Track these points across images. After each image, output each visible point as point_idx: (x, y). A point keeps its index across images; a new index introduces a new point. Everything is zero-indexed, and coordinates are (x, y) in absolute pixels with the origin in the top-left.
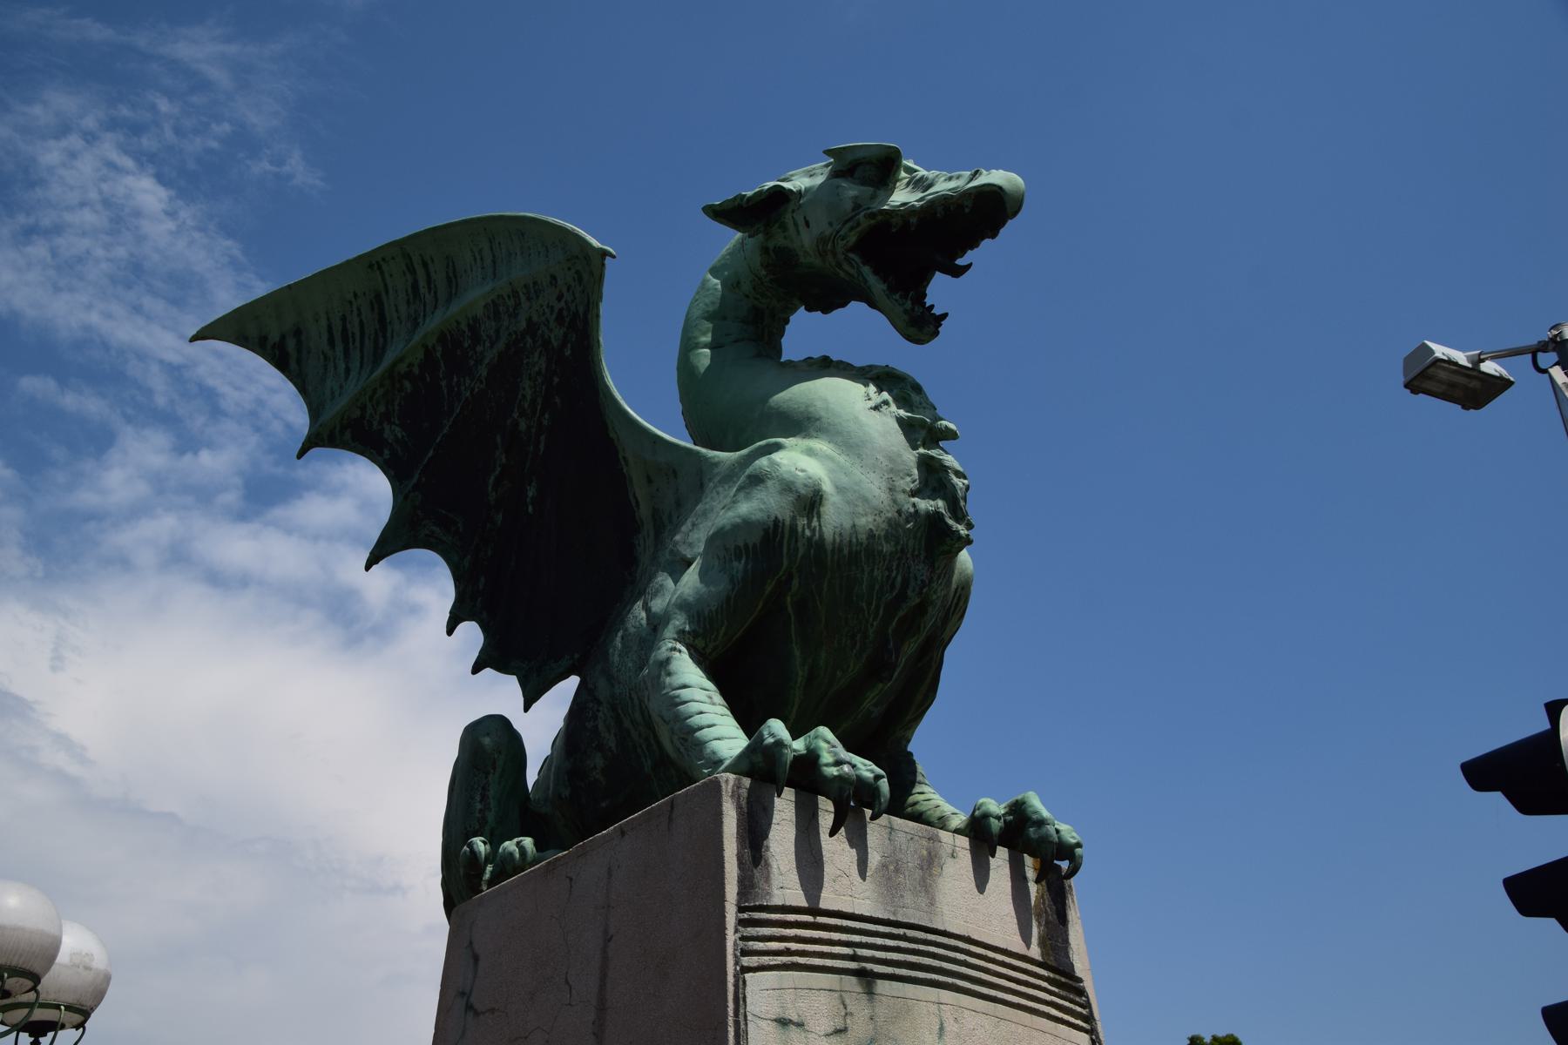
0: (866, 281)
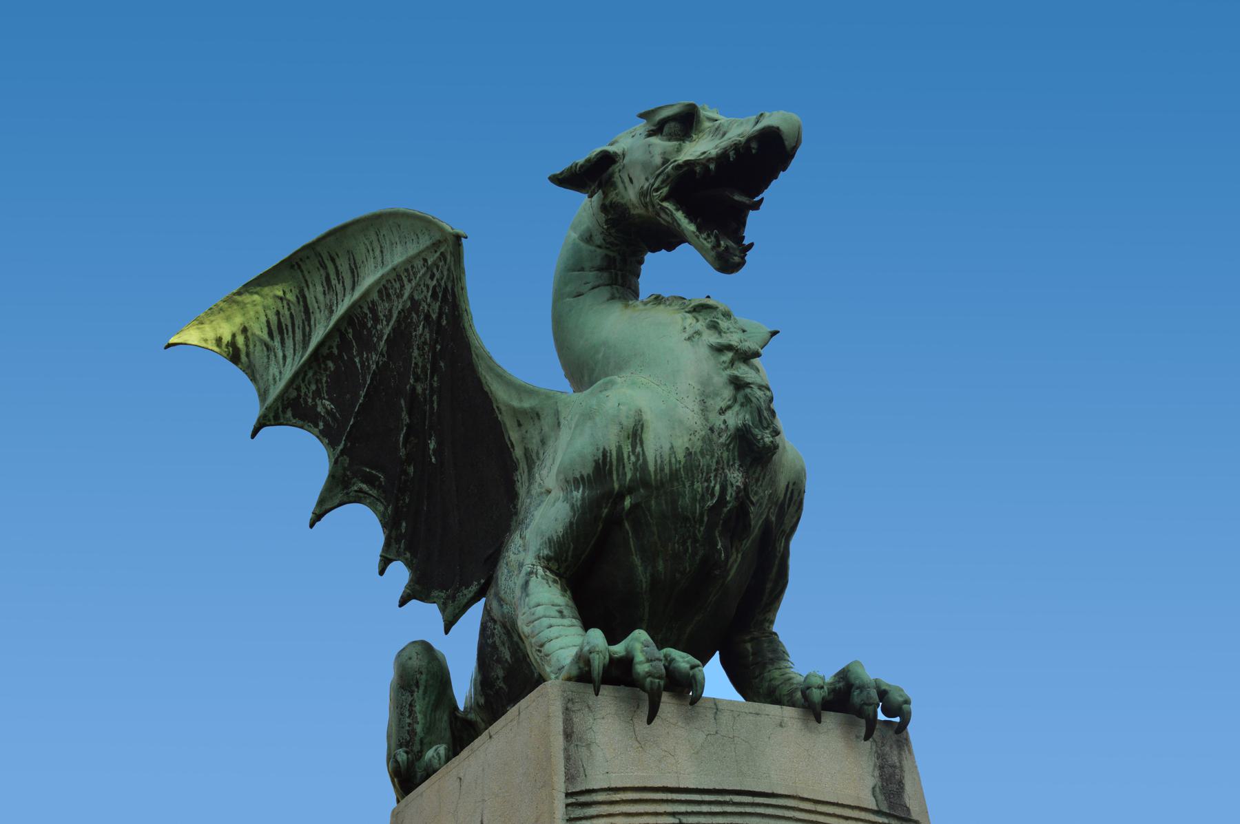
0: (679, 225)
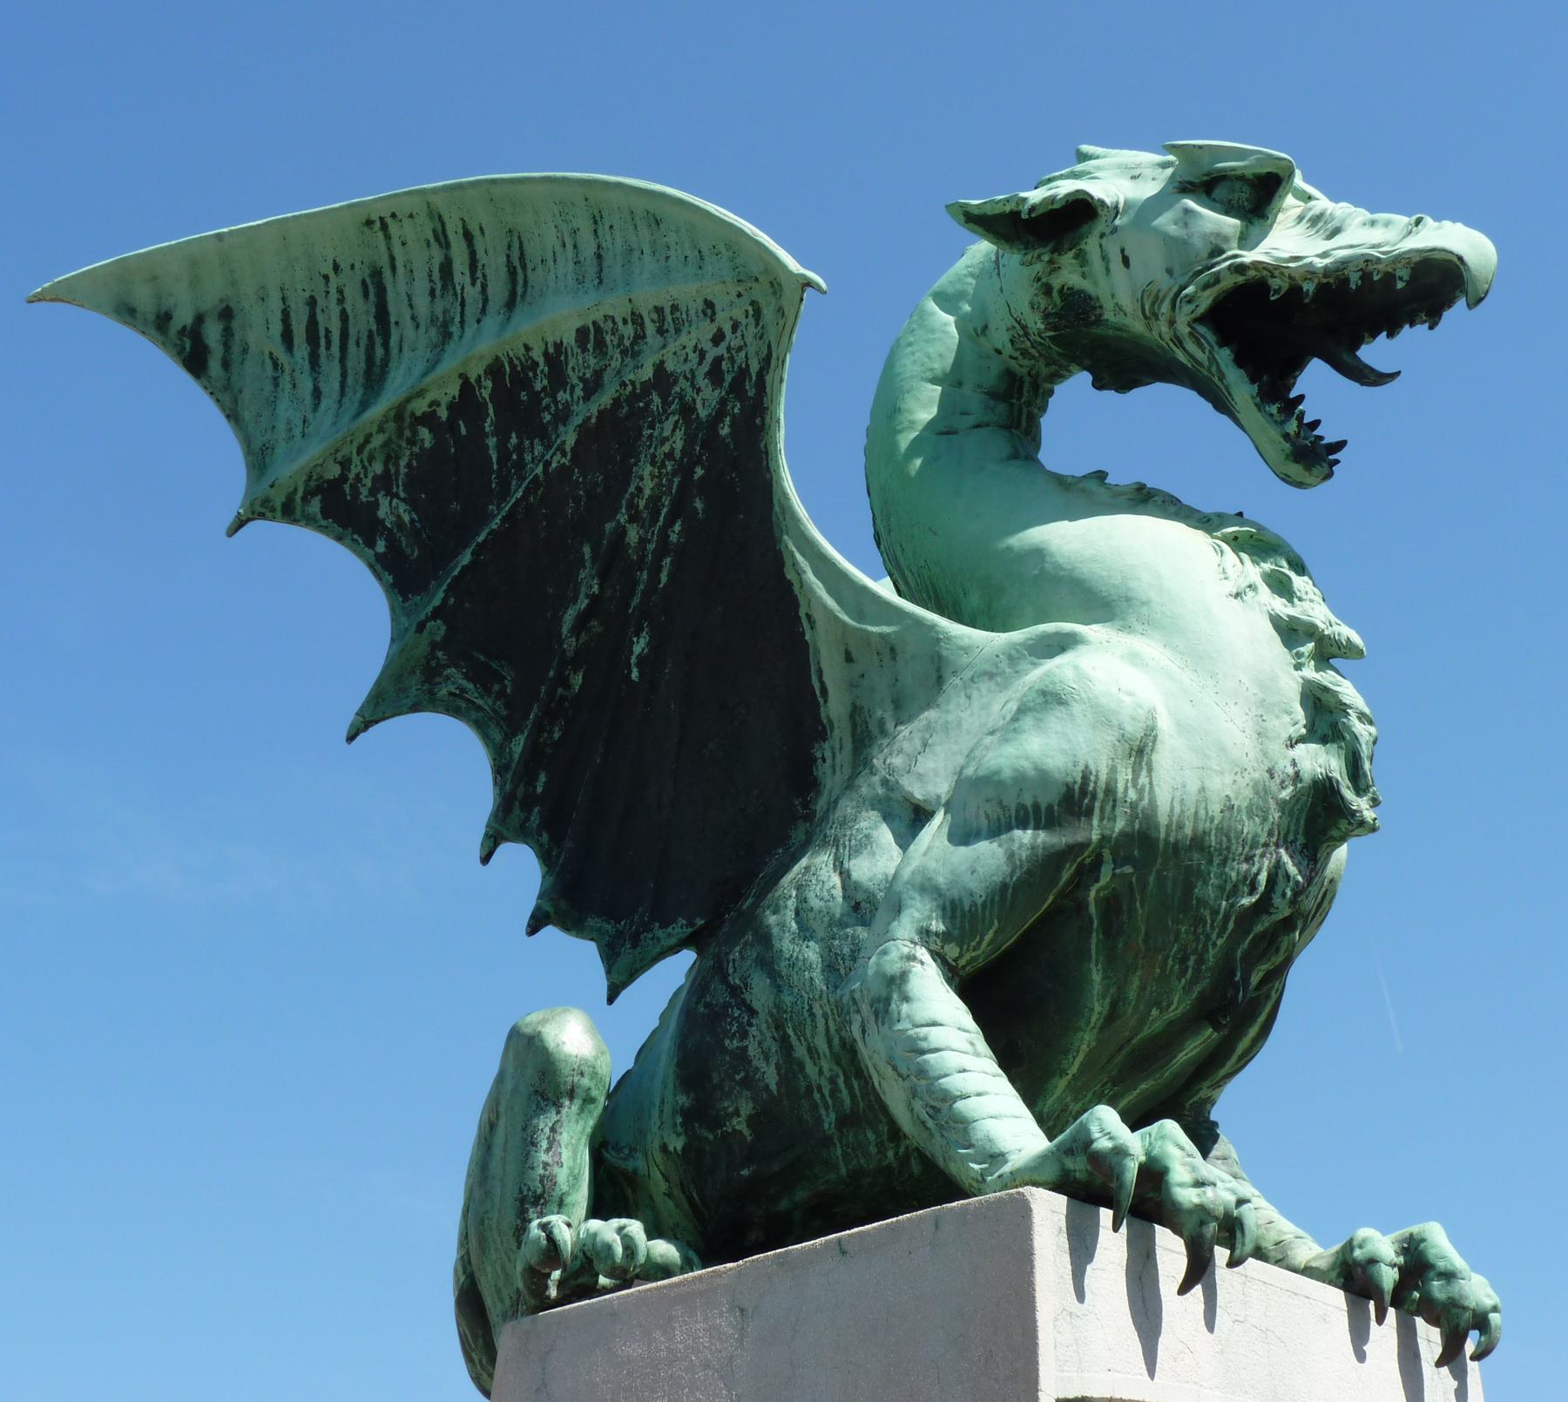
0: (1222, 376)
